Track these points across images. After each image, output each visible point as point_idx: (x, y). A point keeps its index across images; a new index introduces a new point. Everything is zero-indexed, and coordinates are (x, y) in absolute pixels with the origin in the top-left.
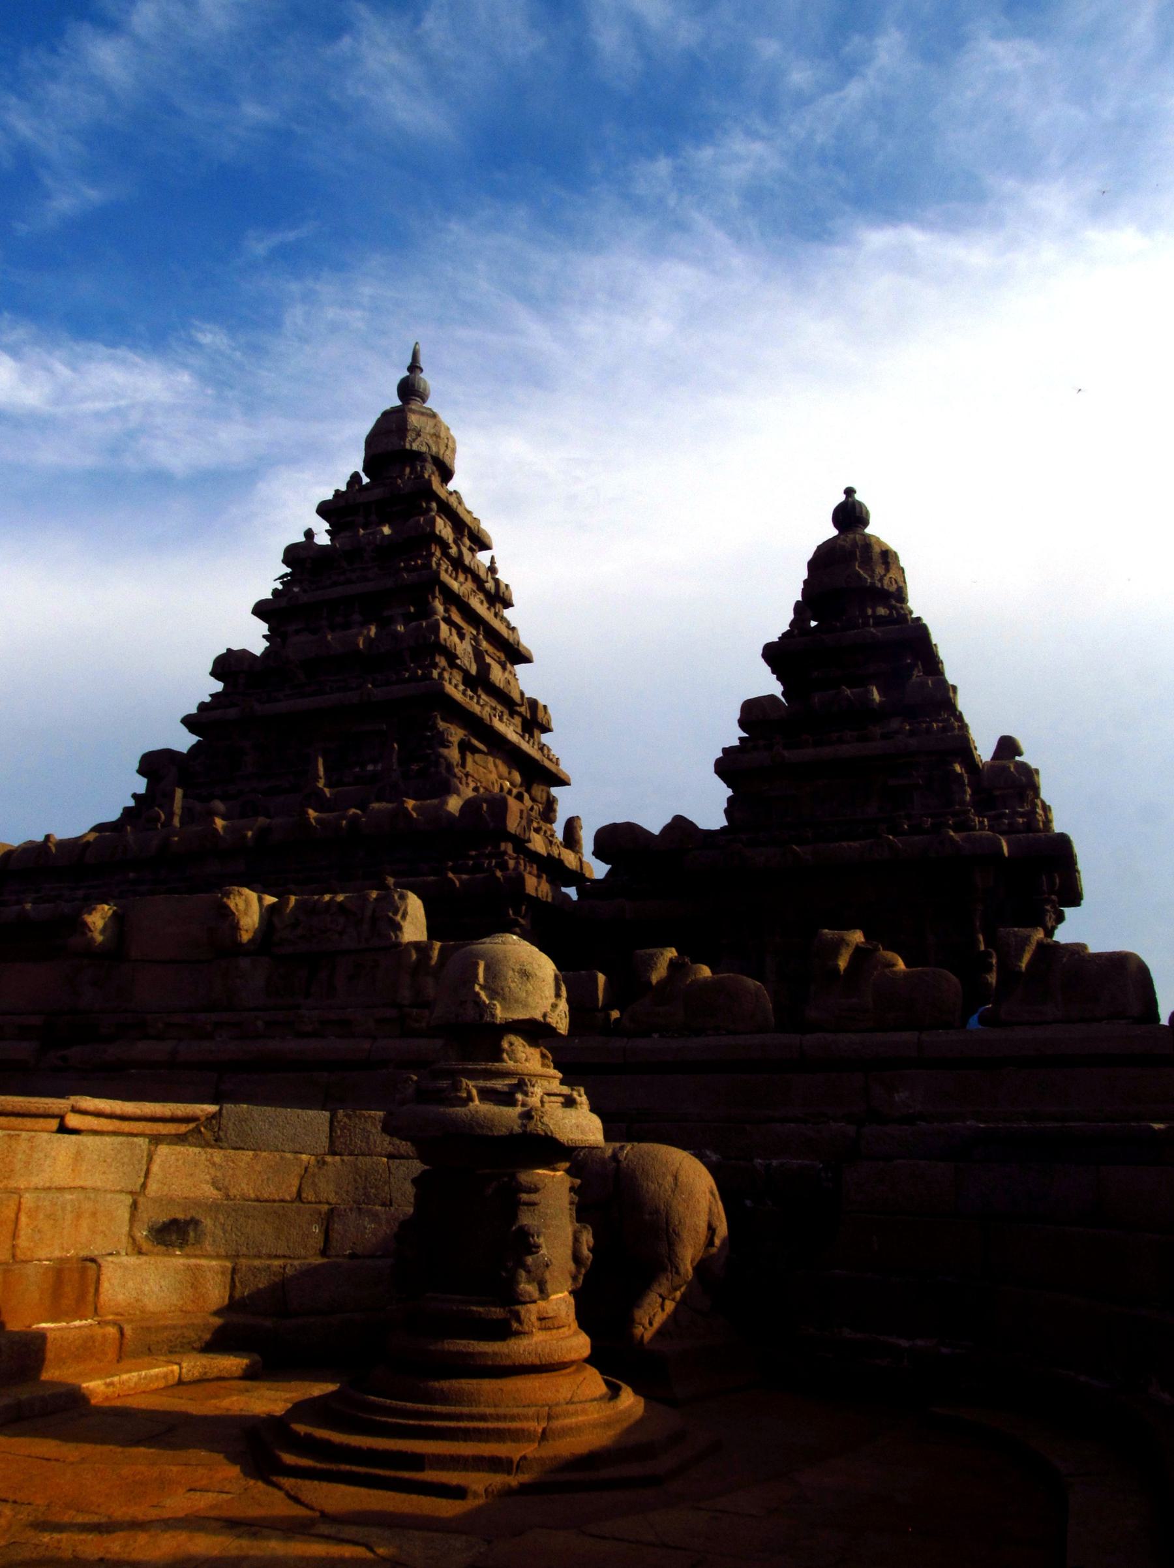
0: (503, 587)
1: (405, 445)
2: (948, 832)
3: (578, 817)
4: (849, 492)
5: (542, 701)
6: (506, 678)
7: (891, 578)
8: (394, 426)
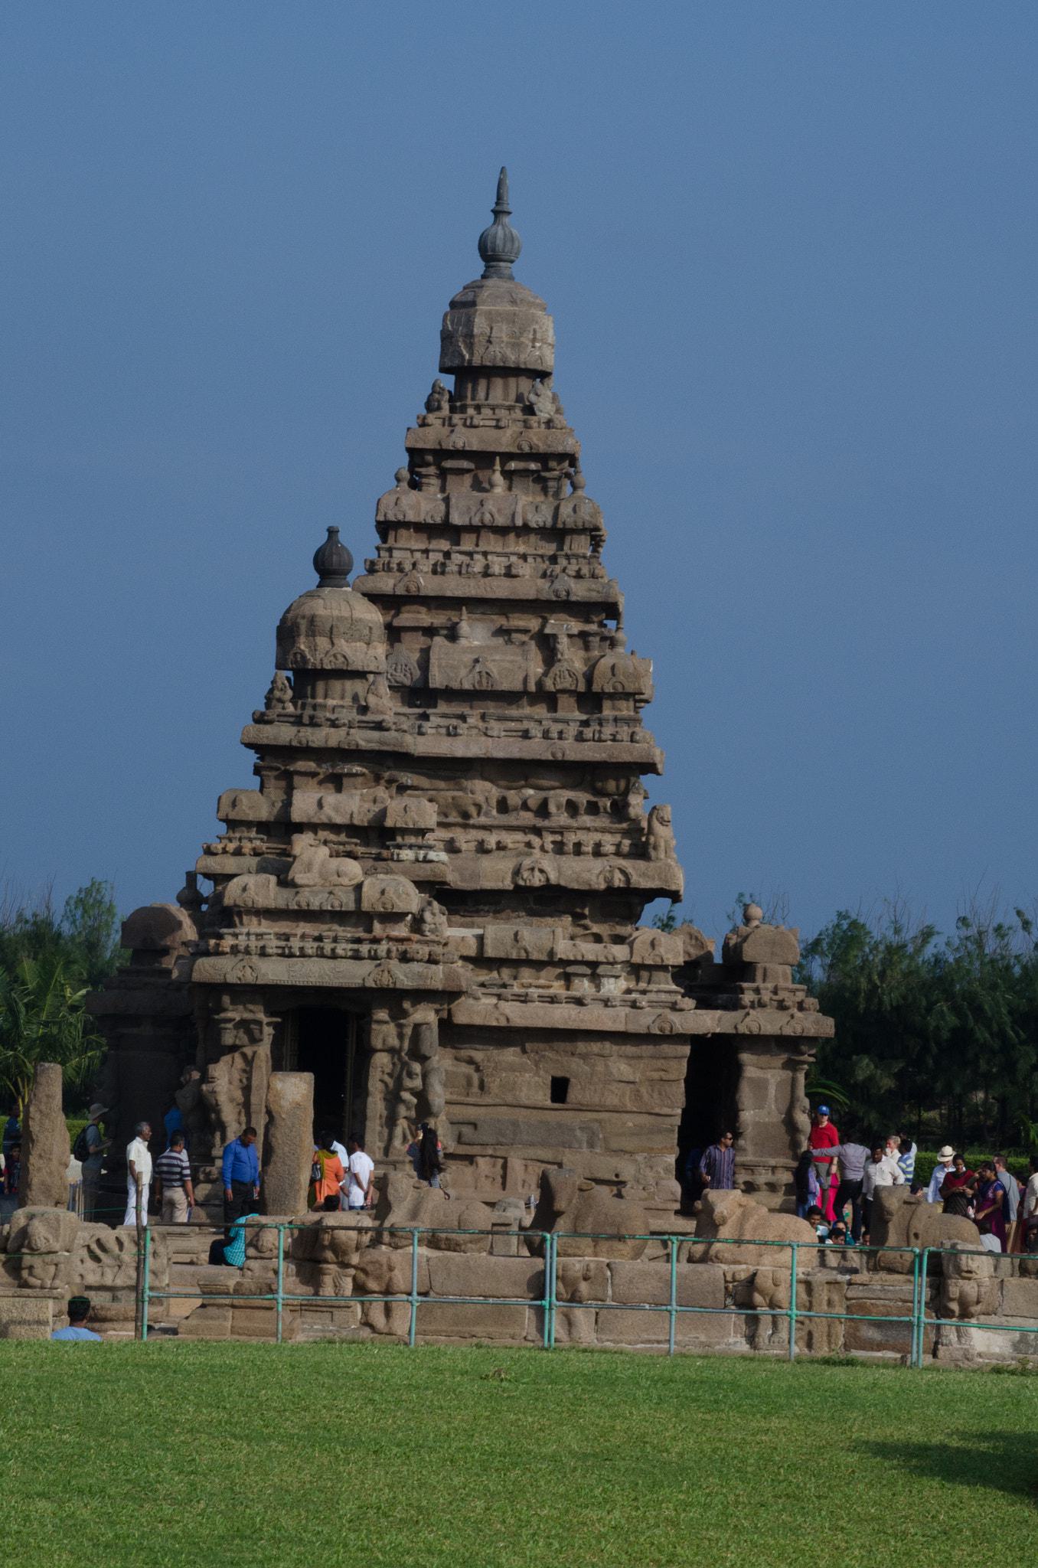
7: (295, 654)
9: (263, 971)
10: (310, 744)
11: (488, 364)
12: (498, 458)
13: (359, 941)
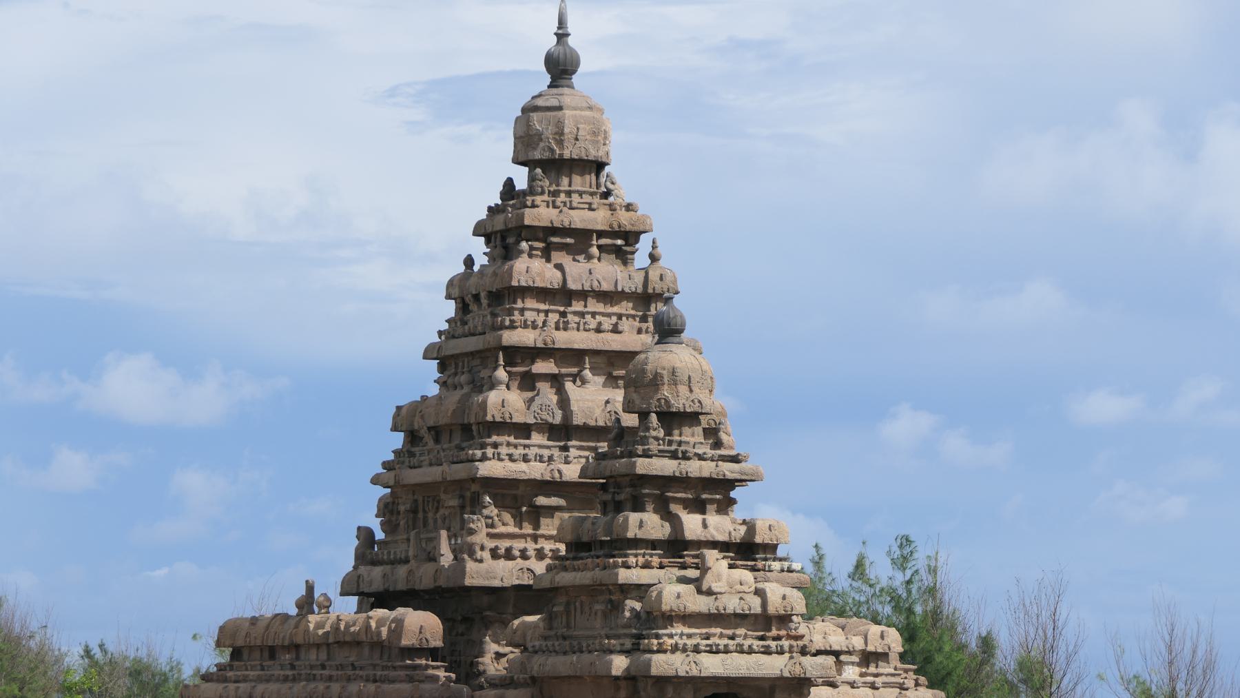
0: (654, 275)
6: (609, 412)
7: (659, 399)
9: (705, 666)
10: (689, 475)
11: (576, 157)
13: (762, 638)
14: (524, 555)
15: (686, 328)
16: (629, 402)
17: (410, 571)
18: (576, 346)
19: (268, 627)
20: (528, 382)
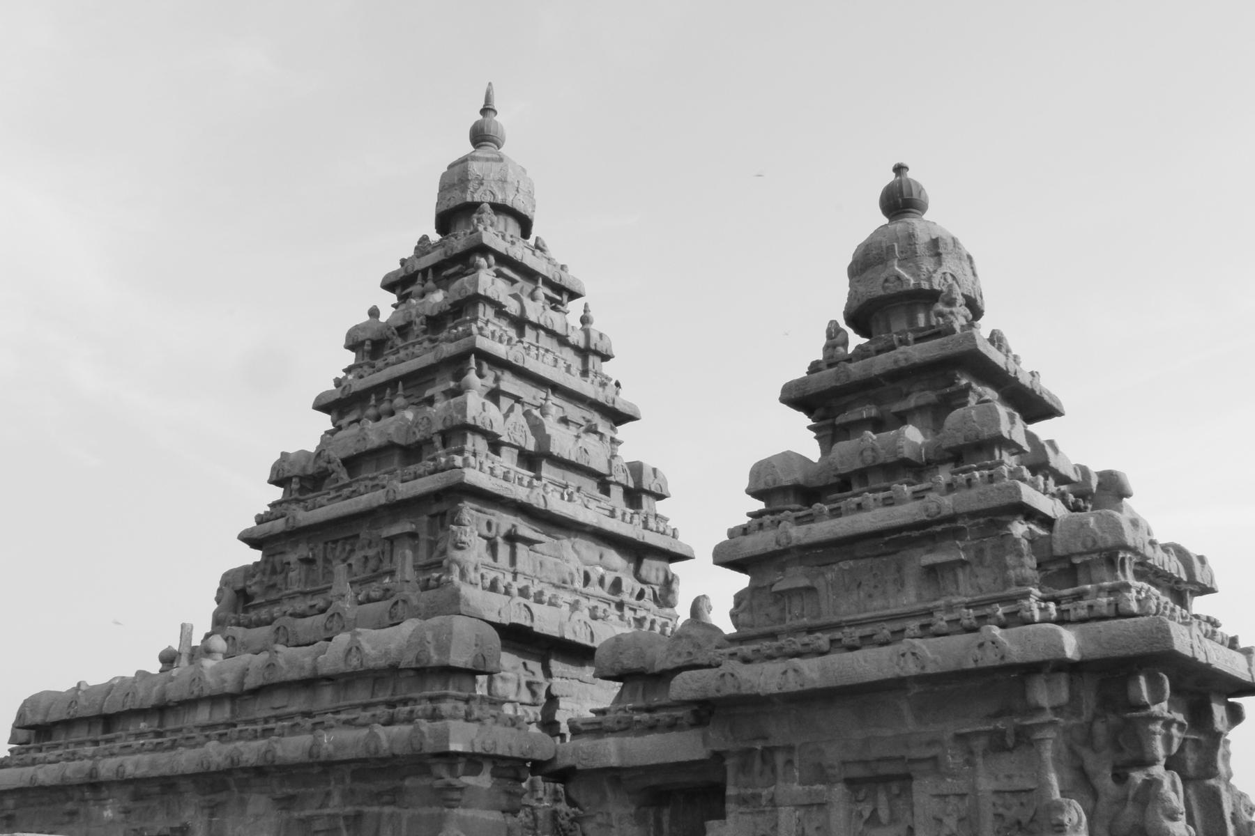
0: (594, 337)
1: (466, 198)
2: (990, 630)
3: (704, 596)
4: (899, 169)
5: (649, 462)
7: (944, 273)
8: (456, 178)
12: (540, 281)
14: (507, 593)
15: (930, 205)
16: (886, 280)
17: (333, 616)
18: (542, 374)
19: (108, 693)
20: (494, 395)
